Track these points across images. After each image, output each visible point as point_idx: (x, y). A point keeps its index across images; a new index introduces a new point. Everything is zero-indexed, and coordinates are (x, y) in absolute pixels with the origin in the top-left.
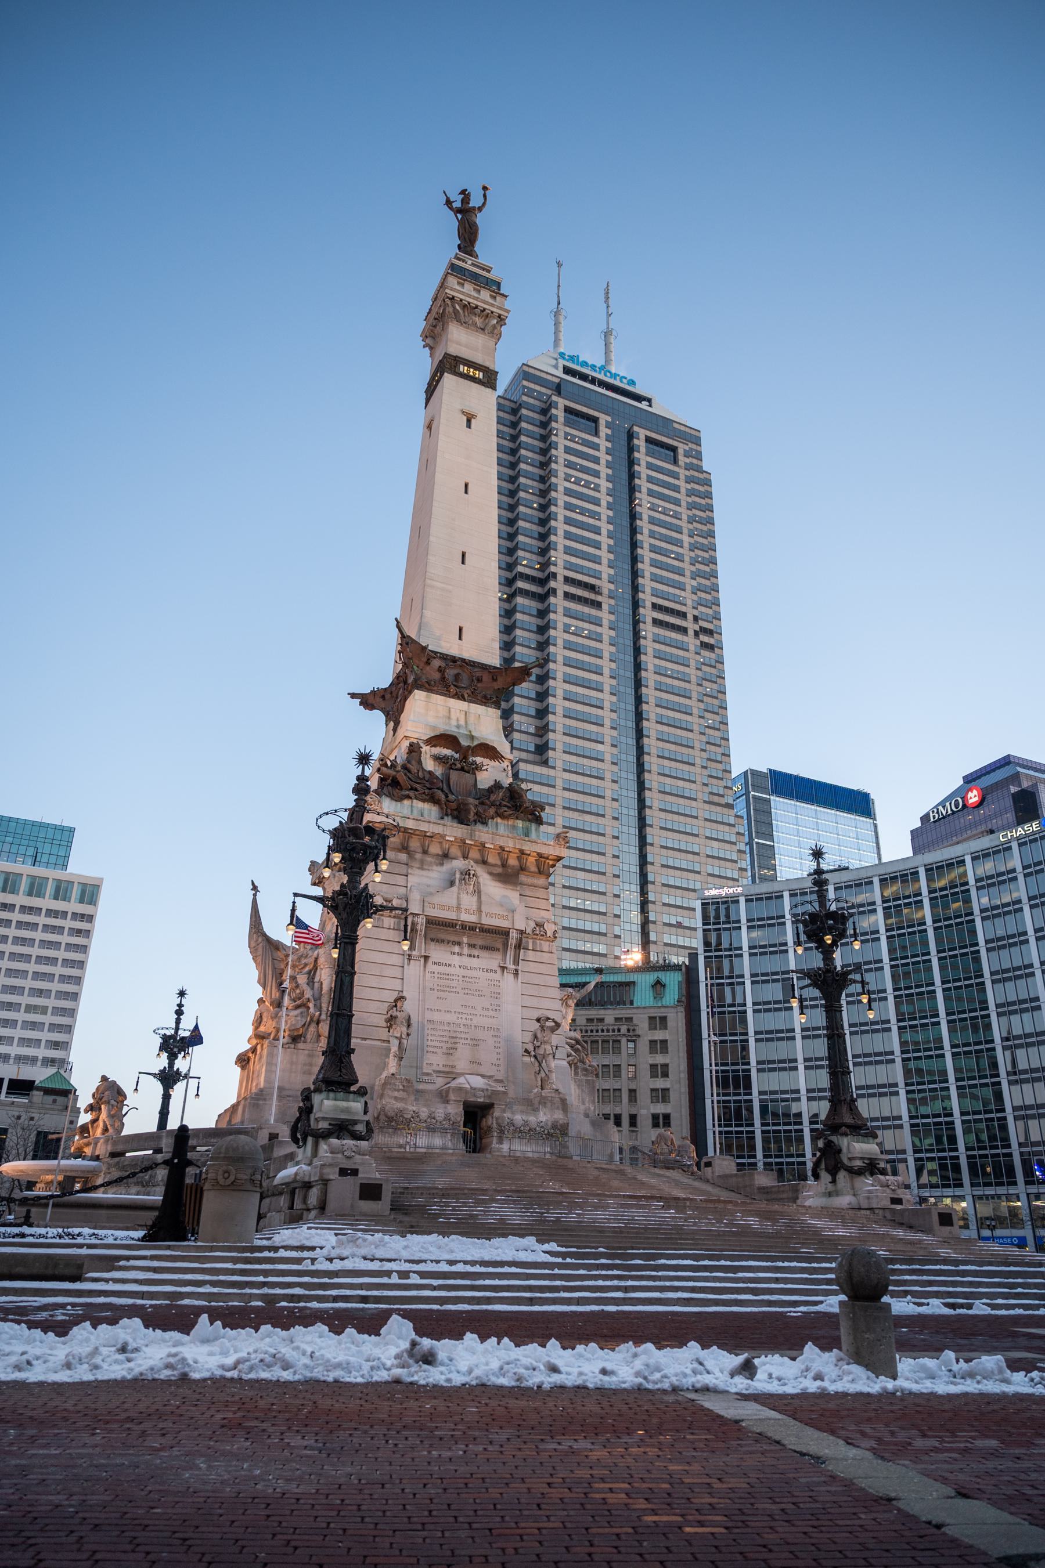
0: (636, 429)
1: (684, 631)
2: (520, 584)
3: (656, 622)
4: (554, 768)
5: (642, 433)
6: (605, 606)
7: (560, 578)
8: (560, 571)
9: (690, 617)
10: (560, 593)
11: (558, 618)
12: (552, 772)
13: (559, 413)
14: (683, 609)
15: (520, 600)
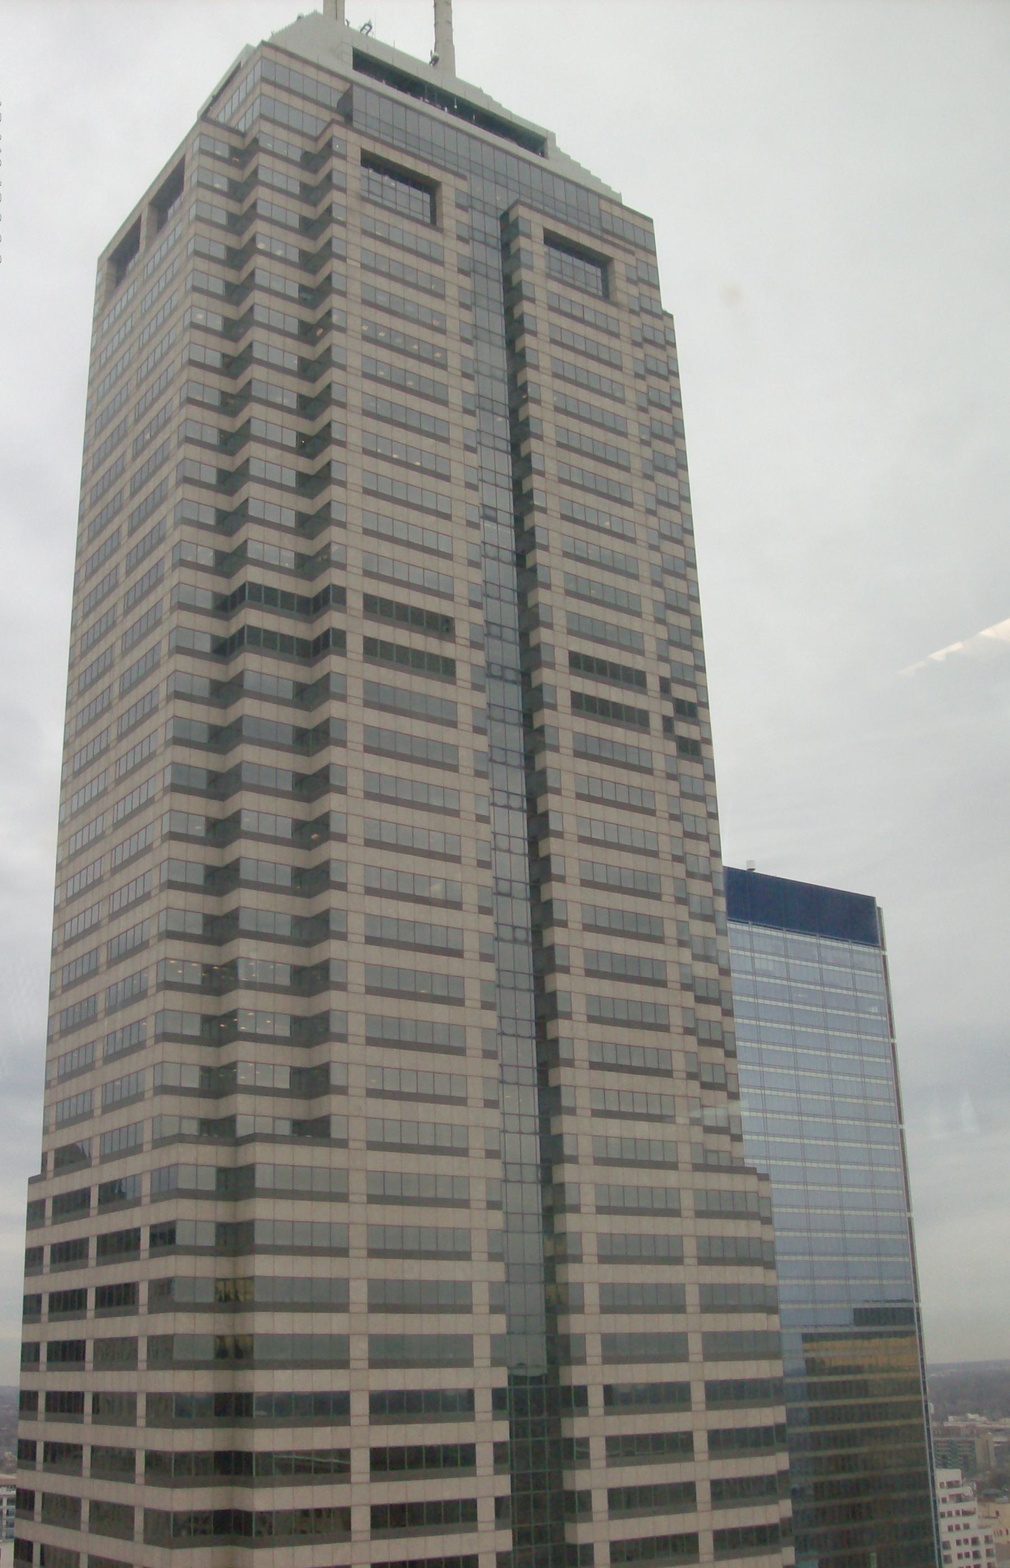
0: (522, 211)
1: (638, 720)
2: (252, 617)
3: (582, 704)
4: (343, 1144)
5: (535, 224)
6: (463, 672)
7: (355, 602)
8: (357, 586)
9: (653, 683)
10: (355, 644)
11: (350, 713)
12: (338, 1158)
13: (347, 170)
14: (637, 663)
15: (252, 663)
